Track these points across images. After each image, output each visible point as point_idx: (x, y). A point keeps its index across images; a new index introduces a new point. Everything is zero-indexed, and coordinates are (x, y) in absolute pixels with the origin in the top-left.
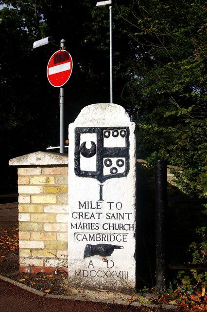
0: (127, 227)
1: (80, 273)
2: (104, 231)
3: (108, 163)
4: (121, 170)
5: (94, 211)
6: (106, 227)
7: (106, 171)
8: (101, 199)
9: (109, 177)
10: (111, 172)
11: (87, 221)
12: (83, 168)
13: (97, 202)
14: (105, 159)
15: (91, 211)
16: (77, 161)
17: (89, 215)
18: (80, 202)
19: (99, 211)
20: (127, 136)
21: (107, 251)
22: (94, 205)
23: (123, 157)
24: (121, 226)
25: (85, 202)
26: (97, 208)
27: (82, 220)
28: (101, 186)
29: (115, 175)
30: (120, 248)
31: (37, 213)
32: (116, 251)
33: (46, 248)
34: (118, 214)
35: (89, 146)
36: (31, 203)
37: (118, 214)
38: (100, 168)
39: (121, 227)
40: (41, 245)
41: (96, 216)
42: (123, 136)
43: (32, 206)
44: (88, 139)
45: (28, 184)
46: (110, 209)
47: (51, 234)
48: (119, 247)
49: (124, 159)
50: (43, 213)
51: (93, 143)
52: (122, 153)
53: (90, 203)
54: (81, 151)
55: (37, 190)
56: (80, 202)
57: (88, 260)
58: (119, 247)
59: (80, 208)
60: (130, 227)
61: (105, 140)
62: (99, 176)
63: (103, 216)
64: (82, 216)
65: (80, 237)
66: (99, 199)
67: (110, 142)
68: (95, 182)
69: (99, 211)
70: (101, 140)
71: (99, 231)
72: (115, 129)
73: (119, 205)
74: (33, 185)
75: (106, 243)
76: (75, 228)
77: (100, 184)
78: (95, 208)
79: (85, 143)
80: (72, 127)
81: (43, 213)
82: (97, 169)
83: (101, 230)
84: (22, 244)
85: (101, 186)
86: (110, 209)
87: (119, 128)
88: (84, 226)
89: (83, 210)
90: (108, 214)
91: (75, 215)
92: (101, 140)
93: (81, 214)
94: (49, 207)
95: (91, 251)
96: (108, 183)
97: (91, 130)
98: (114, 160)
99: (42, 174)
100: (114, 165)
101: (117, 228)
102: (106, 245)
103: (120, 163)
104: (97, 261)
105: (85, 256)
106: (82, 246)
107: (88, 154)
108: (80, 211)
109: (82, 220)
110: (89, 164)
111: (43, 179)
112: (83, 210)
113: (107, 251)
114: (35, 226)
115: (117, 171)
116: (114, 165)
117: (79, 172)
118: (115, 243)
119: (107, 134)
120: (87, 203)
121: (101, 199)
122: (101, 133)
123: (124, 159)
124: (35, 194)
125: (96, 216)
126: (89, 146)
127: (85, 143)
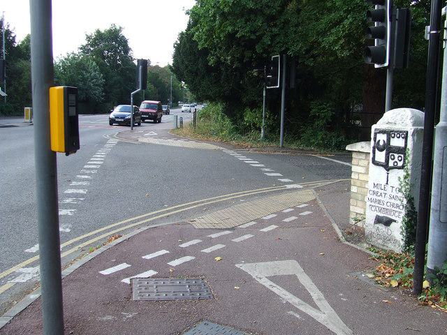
1: (371, 234)
2: (387, 208)
3: (392, 157)
4: (400, 164)
5: (382, 191)
6: (389, 204)
7: (391, 164)
8: (387, 183)
9: (392, 168)
12: (377, 159)
14: (391, 154)
15: (380, 191)
16: (374, 153)
17: (379, 194)
19: (385, 192)
20: (406, 138)
21: (388, 222)
22: (383, 187)
27: (375, 197)
29: (395, 167)
32: (393, 224)
35: (381, 143)
38: (387, 161)
39: (398, 206)
41: (383, 195)
42: (403, 138)
44: (382, 138)
48: (395, 221)
49: (402, 156)
51: (384, 141)
52: (402, 151)
54: (377, 147)
57: (377, 225)
58: (395, 221)
61: (392, 139)
62: (386, 166)
63: (388, 196)
65: (373, 209)
67: (397, 142)
68: (383, 170)
69: (385, 192)
70: (389, 140)
71: (383, 207)
75: (388, 216)
79: (379, 141)
80: (374, 127)
83: (385, 206)
84: (352, 208)
87: (401, 132)
89: (376, 189)
91: (371, 192)
92: (389, 140)
96: (390, 171)
97: (383, 132)
98: (396, 155)
100: (396, 159)
102: (387, 218)
103: (400, 158)
104: (381, 227)
108: (373, 189)
110: (381, 156)
112: (376, 189)
113: (388, 222)
114: (360, 197)
117: (374, 162)
118: (393, 218)
119: (393, 135)
121: (387, 183)
122: (390, 134)
123: (402, 156)
125: (383, 195)
126: (381, 143)
127: (379, 141)
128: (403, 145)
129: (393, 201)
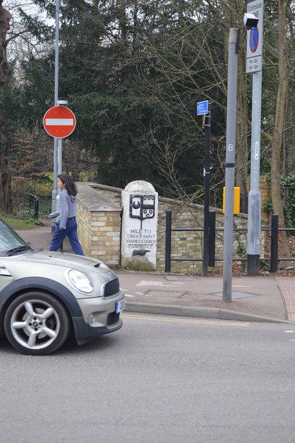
7: (144, 216)
16: (131, 211)
20: (154, 199)
27: (132, 239)
32: (147, 254)
33: (107, 254)
35: (136, 203)
36: (99, 231)
38: (141, 214)
40: (104, 253)
44: (136, 201)
45: (97, 221)
52: (152, 207)
55: (103, 224)
62: (141, 218)
65: (131, 247)
67: (147, 202)
68: (138, 221)
70: (142, 201)
72: (149, 196)
88: (133, 241)
89: (133, 234)
92: (142, 201)
95: (136, 253)
96: (145, 222)
98: (148, 211)
99: (106, 216)
100: (148, 213)
104: (137, 257)
105: (133, 255)
106: (132, 250)
107: (136, 208)
109: (132, 239)
110: (136, 212)
111: (105, 219)
112: (133, 234)
116: (148, 213)
117: (131, 216)
118: (147, 249)
126: (136, 203)
128: (153, 204)
129: (146, 239)
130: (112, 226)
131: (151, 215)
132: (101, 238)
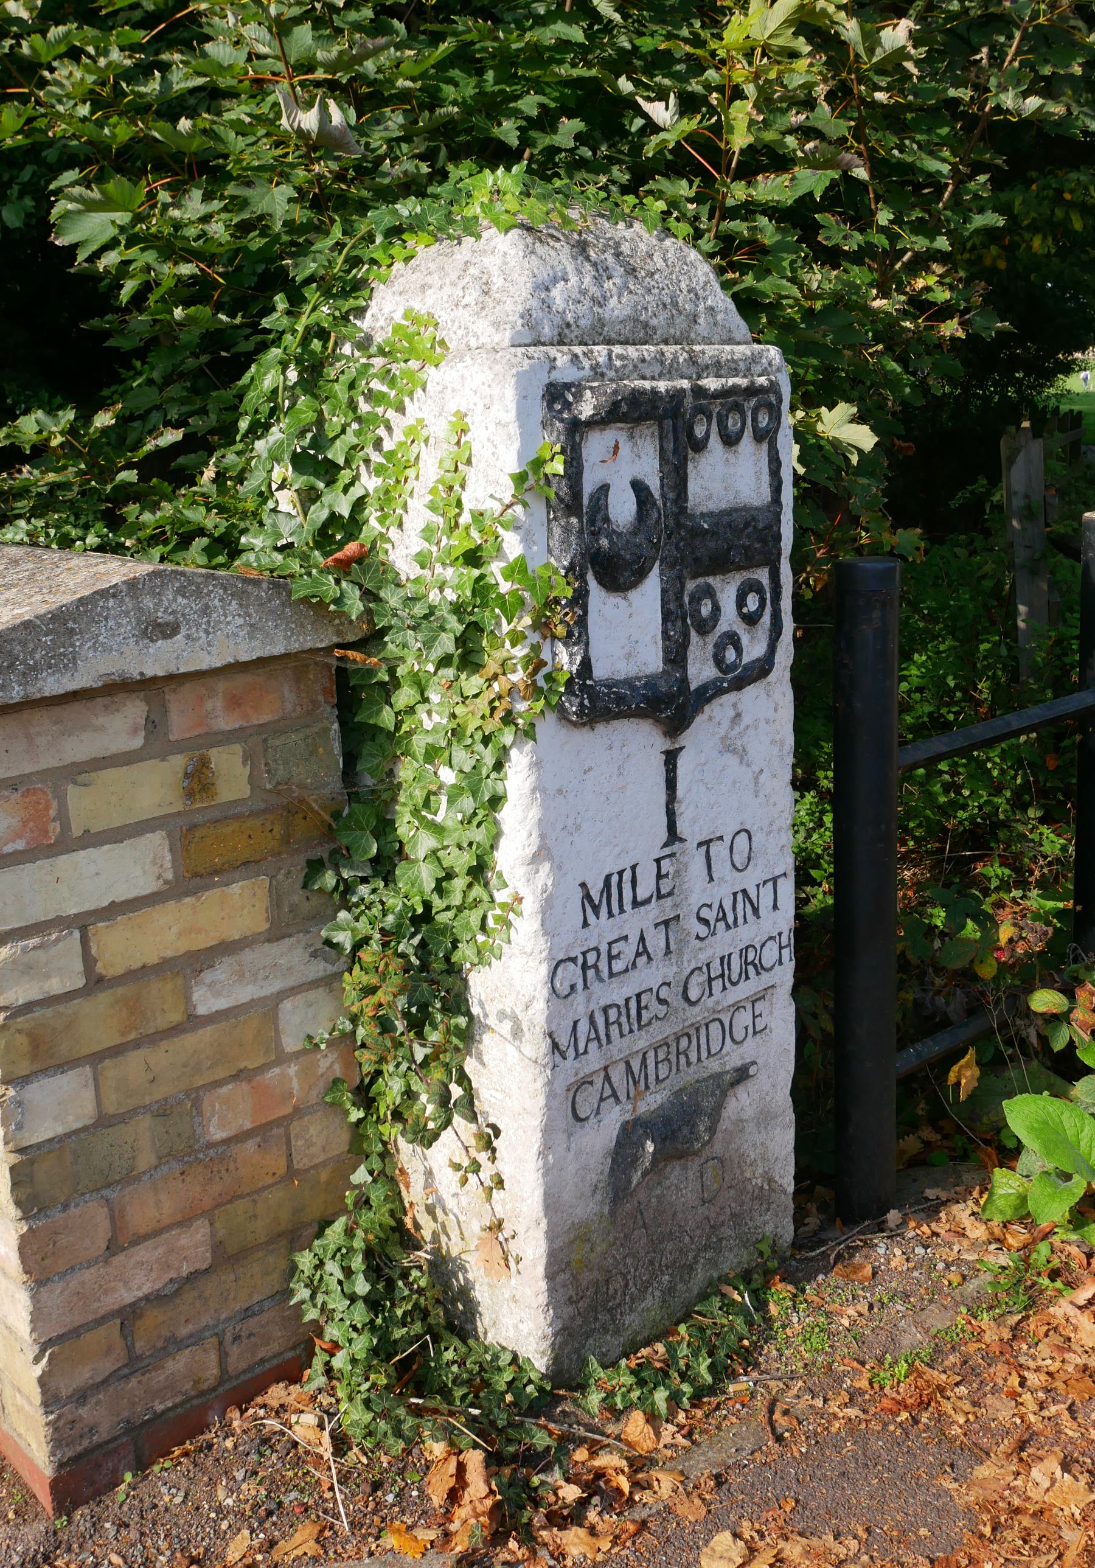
0: (770, 955)
8: (673, 835)
10: (719, 660)
11: (617, 992)
13: (658, 861)
14: (691, 585)
17: (629, 950)
18: (583, 885)
23: (759, 565)
24: (751, 956)
25: (608, 879)
26: (660, 897)
28: (671, 758)
30: (748, 1077)
31: (137, 1044)
34: (740, 897)
36: (95, 982)
37: (740, 897)
43: (104, 998)
46: (711, 879)
47: (251, 1145)
50: (192, 1022)
51: (639, 487)
53: (627, 876)
56: (583, 885)
59: (585, 924)
60: (781, 948)
64: (595, 966)
66: (664, 835)
73: (742, 840)
74: (91, 840)
76: (571, 1053)
77: (667, 745)
78: (648, 901)
79: (604, 489)
81: (192, 1022)
82: (667, 660)
85: (671, 758)
86: (711, 879)
90: (705, 913)
93: (591, 958)
94: (221, 972)
100: (730, 618)
101: (735, 977)
112: (604, 929)
115: (739, 650)
116: (730, 618)
120: (615, 879)
121: (673, 835)
124: (113, 911)
130: (246, 866)
131: (754, 649)
132: (135, 1062)
